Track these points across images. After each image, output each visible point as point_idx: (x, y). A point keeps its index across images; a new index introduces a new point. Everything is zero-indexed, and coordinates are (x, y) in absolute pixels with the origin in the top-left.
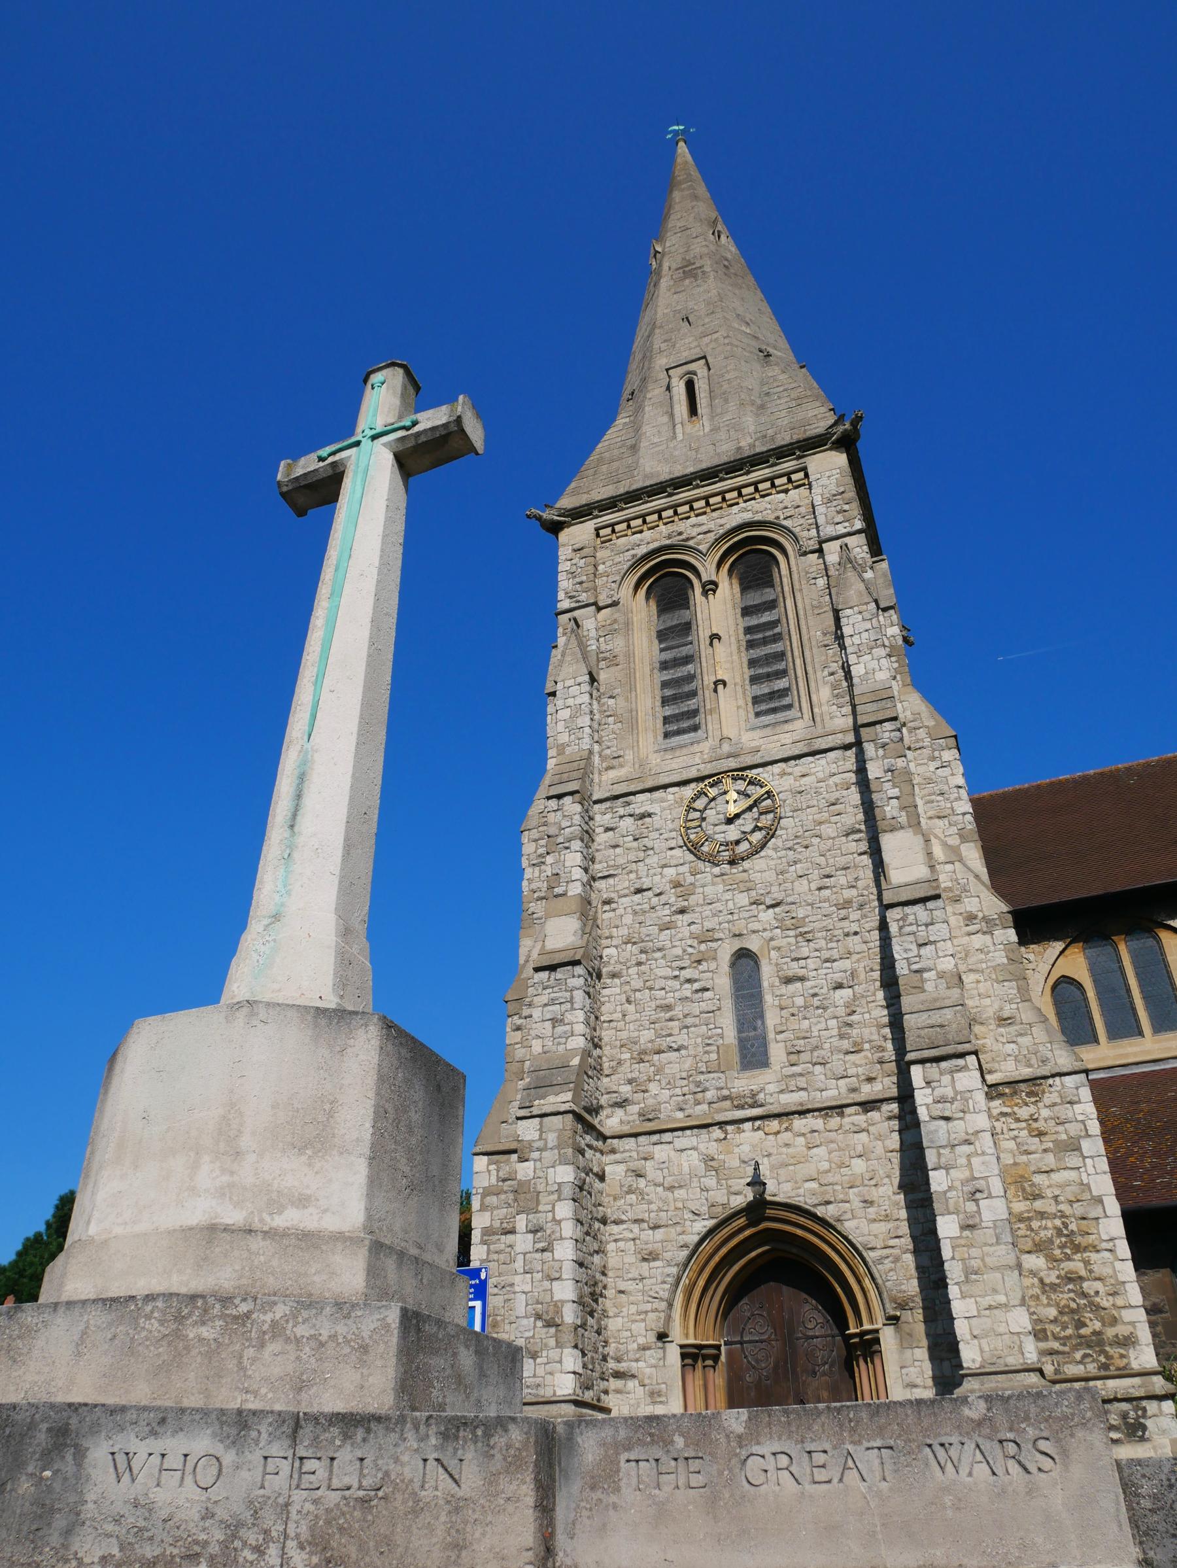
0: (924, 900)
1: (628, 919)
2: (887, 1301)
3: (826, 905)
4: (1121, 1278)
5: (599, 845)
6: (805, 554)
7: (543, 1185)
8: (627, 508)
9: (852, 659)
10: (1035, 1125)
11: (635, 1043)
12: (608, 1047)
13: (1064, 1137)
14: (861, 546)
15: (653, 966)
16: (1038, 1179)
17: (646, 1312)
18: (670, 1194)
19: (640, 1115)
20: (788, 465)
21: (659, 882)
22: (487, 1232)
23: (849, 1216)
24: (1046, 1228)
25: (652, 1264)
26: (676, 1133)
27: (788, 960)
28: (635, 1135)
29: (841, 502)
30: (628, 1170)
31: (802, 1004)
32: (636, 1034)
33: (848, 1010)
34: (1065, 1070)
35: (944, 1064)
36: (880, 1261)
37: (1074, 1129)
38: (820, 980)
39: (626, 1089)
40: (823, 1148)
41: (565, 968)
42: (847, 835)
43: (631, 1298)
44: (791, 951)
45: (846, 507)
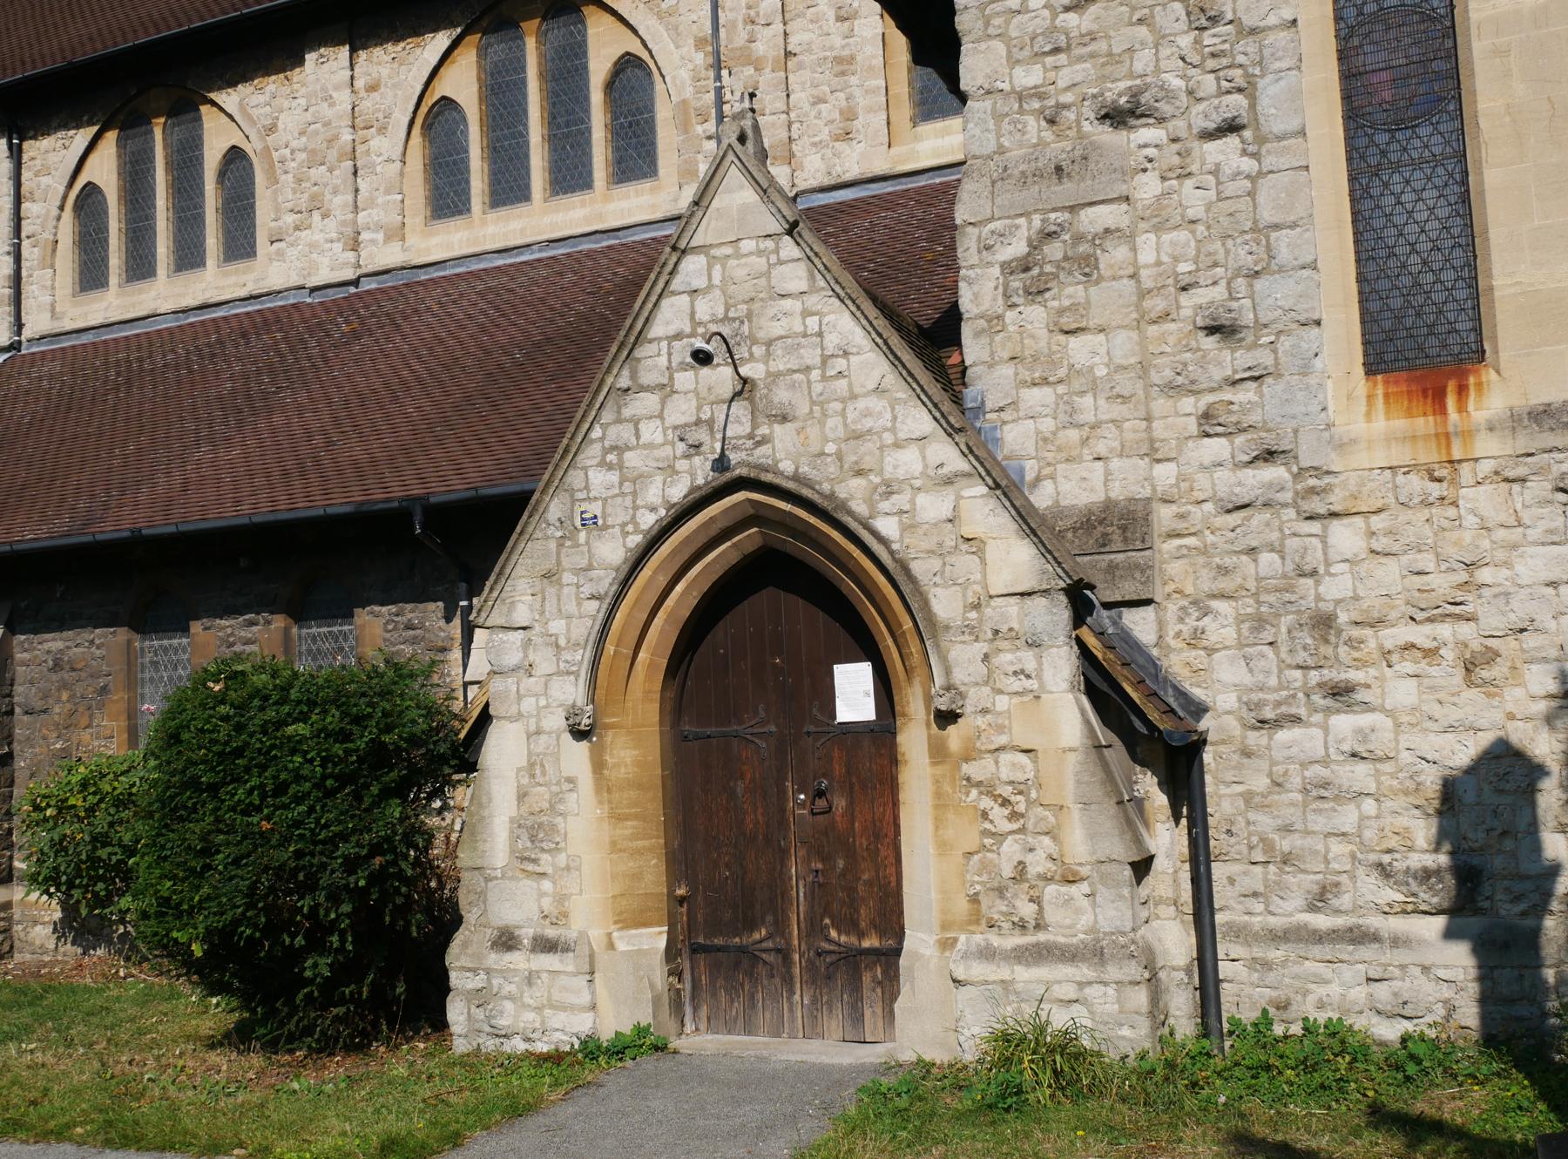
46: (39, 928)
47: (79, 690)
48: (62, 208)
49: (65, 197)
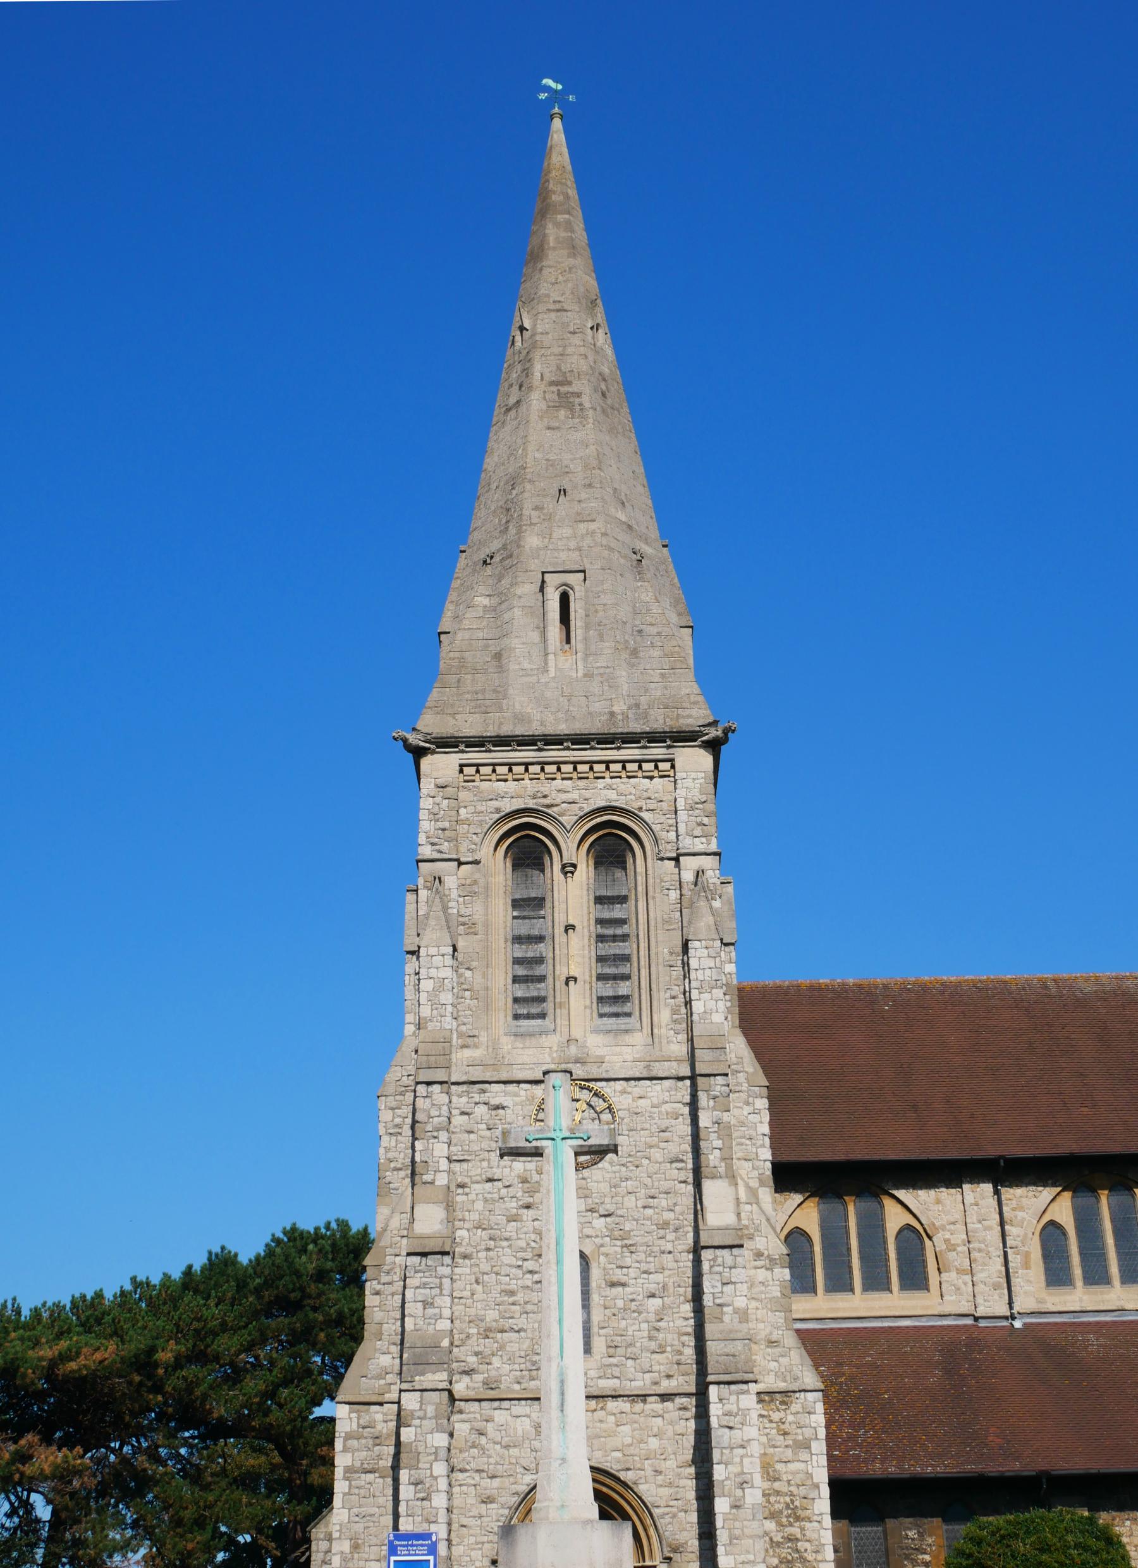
0: (731, 1247)
1: (479, 1205)
2: (664, 1546)
3: (649, 1223)
4: (823, 1541)
5: (455, 1127)
6: (662, 859)
7: (423, 1447)
8: (495, 751)
9: (695, 994)
10: (782, 1427)
11: (482, 1321)
12: (458, 1321)
13: (801, 1438)
14: (714, 870)
15: (500, 1254)
17: (483, 1543)
18: (506, 1452)
19: (484, 1383)
20: (657, 751)
22: (348, 1470)
23: (643, 1481)
24: (779, 1502)
25: (489, 1506)
26: (513, 1402)
27: (614, 1266)
28: (480, 1400)
29: (702, 814)
30: (471, 1429)
31: (622, 1306)
32: (483, 1312)
33: (658, 1318)
34: (809, 1388)
35: (733, 1387)
36: (663, 1516)
37: (808, 1433)
38: (638, 1286)
39: (472, 1360)
40: (629, 1426)
41: (436, 1256)
42: (671, 1162)
43: (471, 1532)
44: (618, 1259)
45: (706, 820)
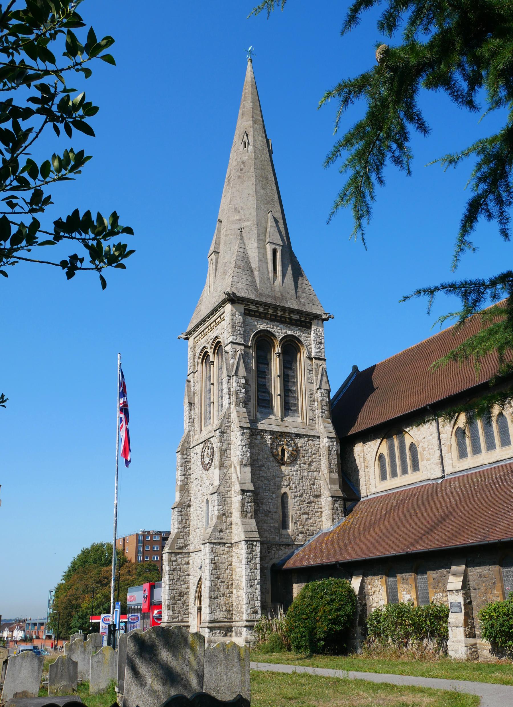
16: (237, 569)
21: (198, 476)
46: (485, 651)
47: (487, 583)
48: (451, 435)
49: (452, 432)
